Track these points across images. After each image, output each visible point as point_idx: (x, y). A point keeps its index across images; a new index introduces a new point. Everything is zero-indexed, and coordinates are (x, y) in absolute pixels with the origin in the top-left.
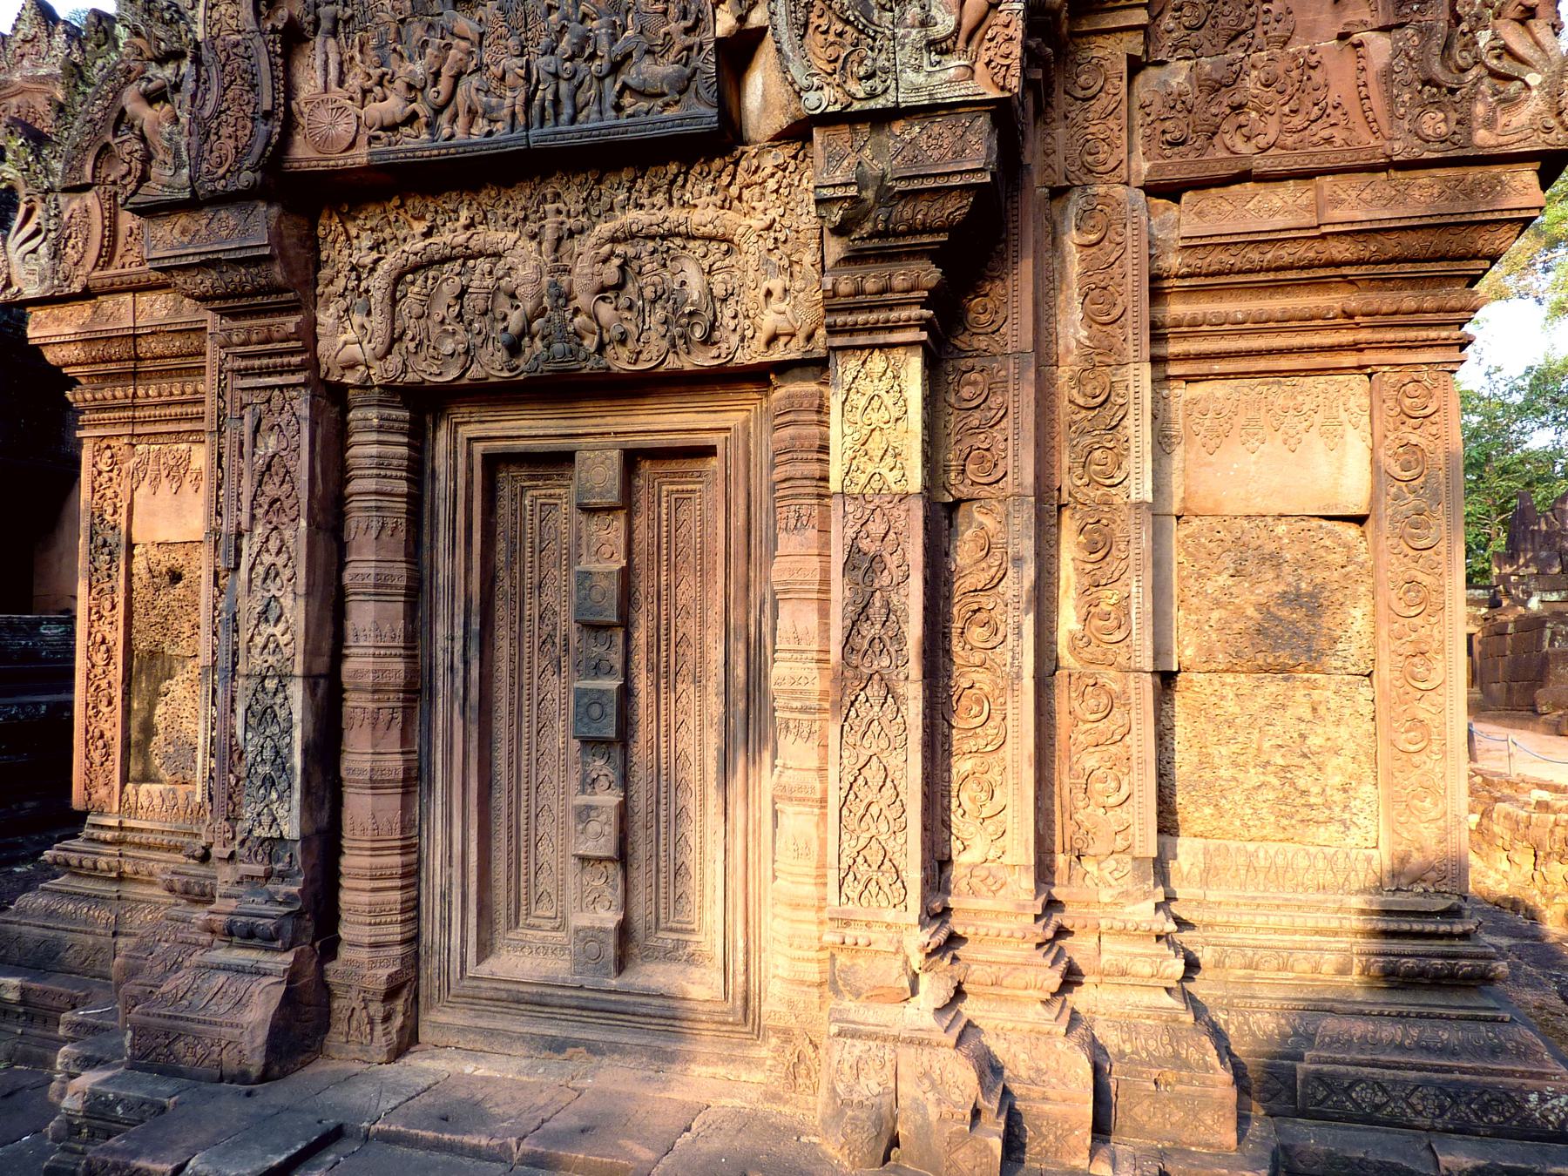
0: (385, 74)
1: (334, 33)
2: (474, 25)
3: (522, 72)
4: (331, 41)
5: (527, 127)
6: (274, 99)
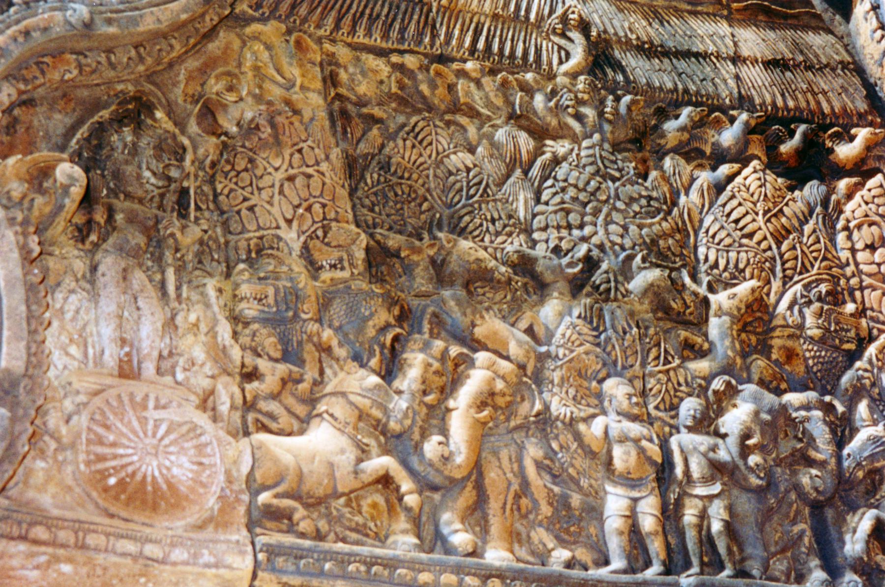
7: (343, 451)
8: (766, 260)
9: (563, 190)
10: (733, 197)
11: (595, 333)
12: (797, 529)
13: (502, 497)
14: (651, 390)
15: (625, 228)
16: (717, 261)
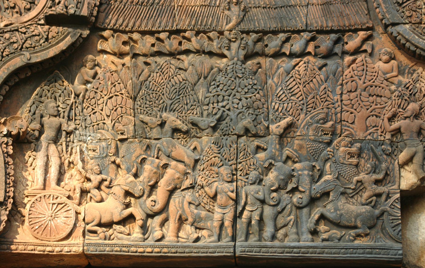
0: (103, 180)
1: (56, 140)
2: (190, 152)
3: (233, 195)
4: (53, 147)
5: (234, 238)
6: (6, 192)
7: (116, 208)
8: (300, 105)
9: (218, 86)
10: (292, 77)
11: (218, 149)
12: (289, 218)
13: (175, 216)
14: (239, 169)
15: (240, 100)
16: (278, 109)
